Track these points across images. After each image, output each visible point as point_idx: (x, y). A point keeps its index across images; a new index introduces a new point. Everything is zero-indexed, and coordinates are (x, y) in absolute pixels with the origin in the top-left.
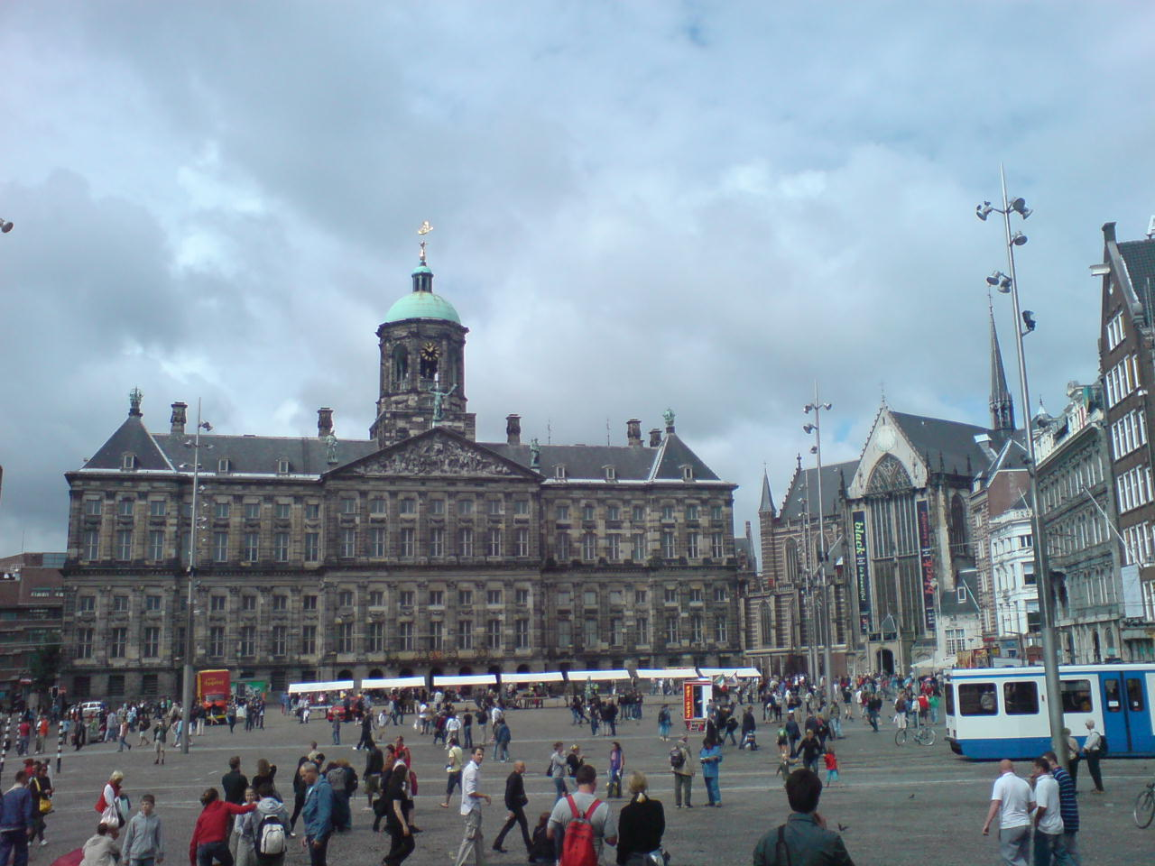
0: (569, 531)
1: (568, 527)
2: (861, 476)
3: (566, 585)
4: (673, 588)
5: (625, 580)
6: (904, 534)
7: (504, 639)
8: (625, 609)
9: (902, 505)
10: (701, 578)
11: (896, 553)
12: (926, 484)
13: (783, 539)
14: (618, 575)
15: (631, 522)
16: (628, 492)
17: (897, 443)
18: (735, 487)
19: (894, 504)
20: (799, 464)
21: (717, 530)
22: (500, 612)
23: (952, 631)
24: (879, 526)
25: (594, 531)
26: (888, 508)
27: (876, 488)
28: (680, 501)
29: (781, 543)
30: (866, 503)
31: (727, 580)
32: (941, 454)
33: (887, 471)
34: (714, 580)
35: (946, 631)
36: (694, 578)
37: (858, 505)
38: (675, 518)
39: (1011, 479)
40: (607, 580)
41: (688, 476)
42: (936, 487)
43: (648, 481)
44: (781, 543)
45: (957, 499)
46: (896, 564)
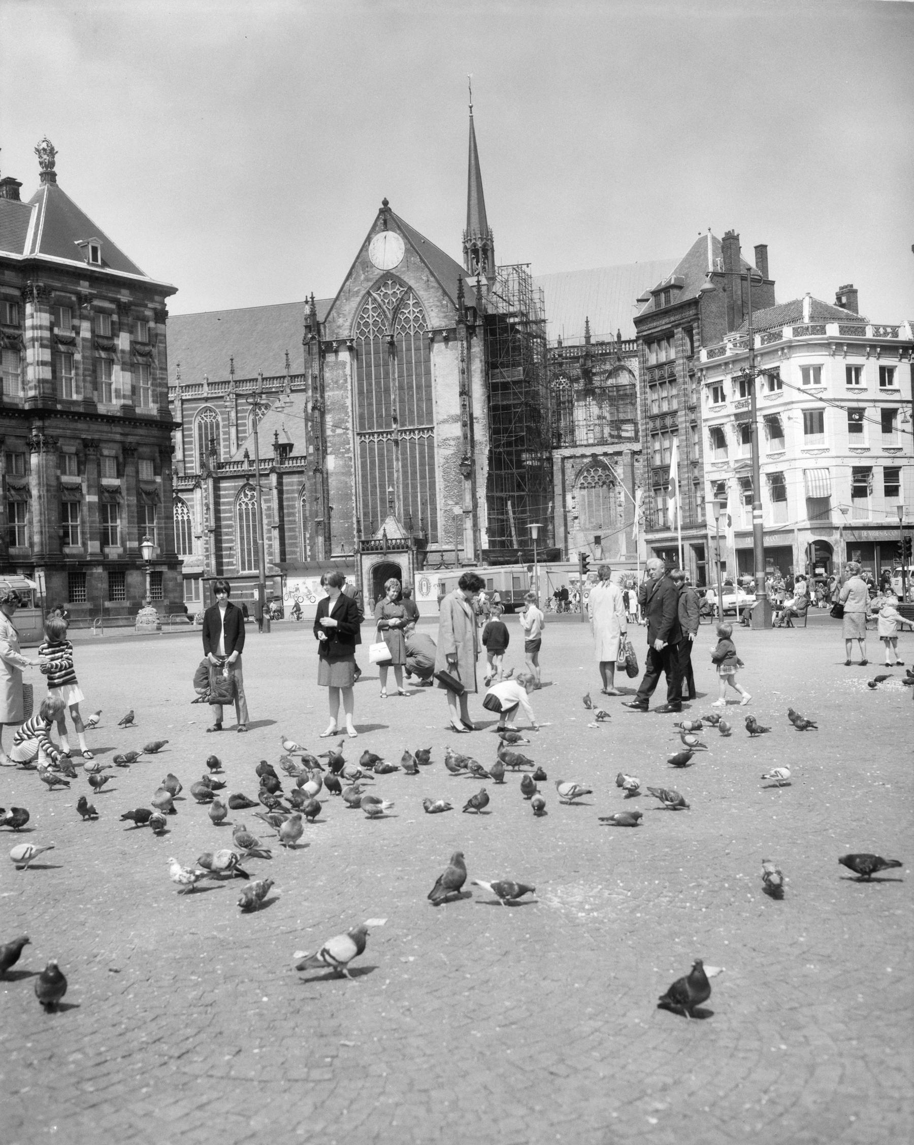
10: (118, 437)
17: (406, 261)
18: (171, 291)
31: (159, 446)
34: (138, 444)
43: (26, 254)
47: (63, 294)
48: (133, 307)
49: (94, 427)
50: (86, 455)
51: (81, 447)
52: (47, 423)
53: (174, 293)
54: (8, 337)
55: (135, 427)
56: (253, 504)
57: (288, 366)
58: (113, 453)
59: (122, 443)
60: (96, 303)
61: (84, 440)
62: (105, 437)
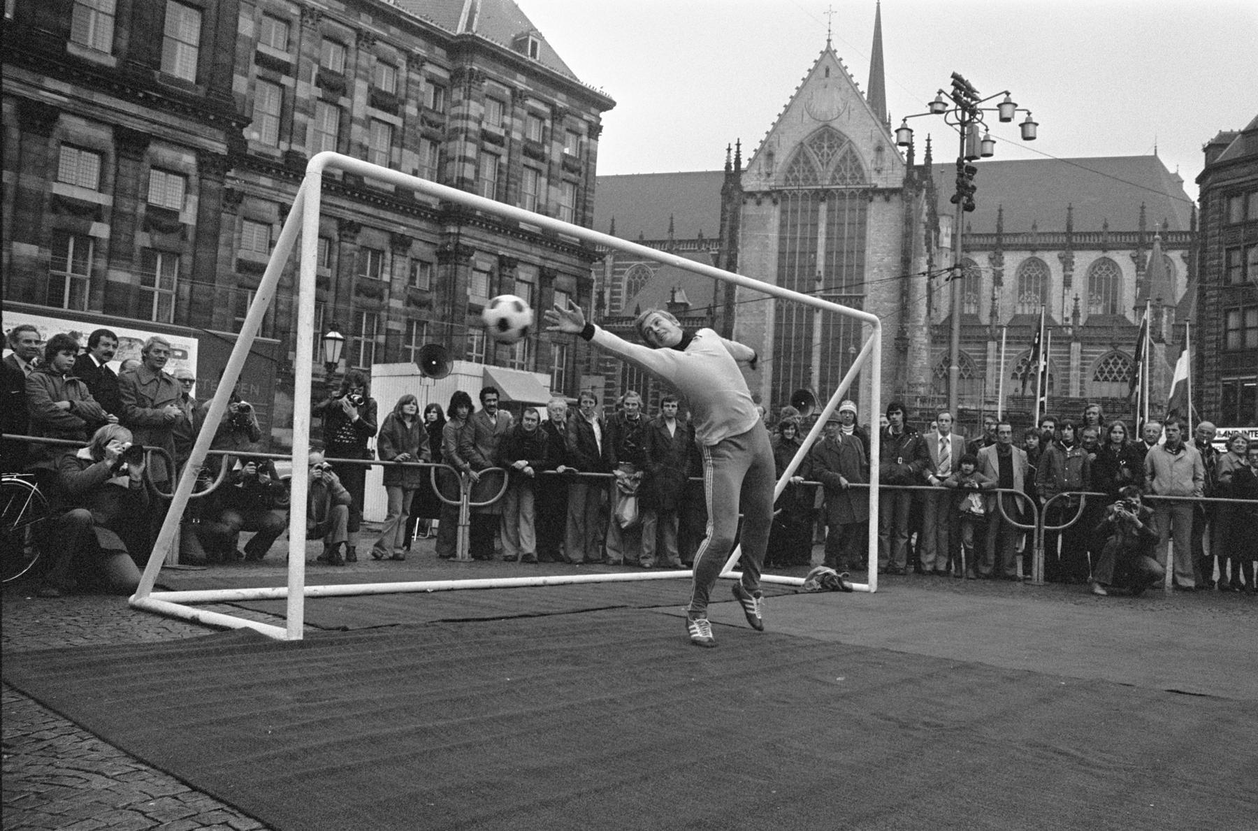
0: (285, 80)
1: (285, 68)
2: (770, 155)
3: (265, 205)
4: (487, 267)
5: (394, 229)
7: (101, 293)
8: (387, 291)
10: (537, 260)
14: (382, 214)
15: (419, 109)
16: (421, 42)
18: (607, 104)
21: (572, 176)
22: (95, 212)
25: (343, 101)
27: (796, 179)
28: (518, 96)
30: (775, 202)
31: (578, 277)
34: (557, 271)
37: (759, 203)
38: (503, 126)
40: (358, 219)
42: (920, 189)
47: (497, 85)
48: (568, 116)
49: (512, 244)
50: (501, 276)
51: (496, 265)
52: (464, 230)
53: (611, 108)
54: (430, 123)
55: (556, 250)
57: (671, 230)
58: (529, 278)
59: (541, 268)
60: (530, 102)
61: (501, 258)
62: (523, 257)
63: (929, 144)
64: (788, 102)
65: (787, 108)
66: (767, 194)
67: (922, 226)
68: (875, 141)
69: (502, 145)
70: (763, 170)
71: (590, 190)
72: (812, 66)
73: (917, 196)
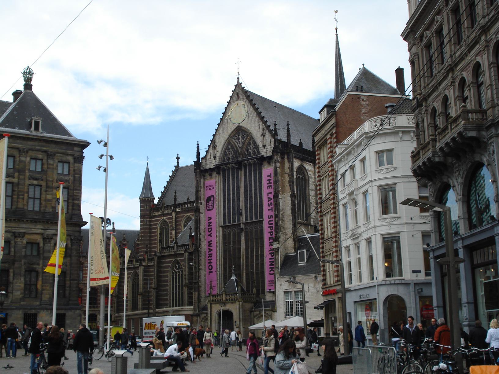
2: (215, 148)
6: (251, 201)
9: (250, 172)
10: (40, 231)
11: (243, 219)
12: (273, 152)
13: (158, 220)
17: (248, 115)
19: (243, 172)
20: (178, 162)
23: (292, 291)
24: (229, 195)
26: (238, 177)
27: (228, 159)
29: (156, 225)
30: (218, 173)
32: (288, 125)
33: (239, 143)
35: (285, 292)
36: (34, 231)
37: (211, 175)
39: (363, 103)
41: (37, 128)
44: (156, 225)
45: (301, 169)
46: (242, 229)
48: (57, 155)
56: (179, 272)
59: (42, 234)
61: (14, 233)
63: (288, 127)
64: (221, 116)
65: (221, 119)
66: (212, 170)
67: (286, 176)
68: (261, 130)
69: (14, 177)
70: (212, 156)
71: (76, 190)
72: (231, 94)
73: (283, 158)
